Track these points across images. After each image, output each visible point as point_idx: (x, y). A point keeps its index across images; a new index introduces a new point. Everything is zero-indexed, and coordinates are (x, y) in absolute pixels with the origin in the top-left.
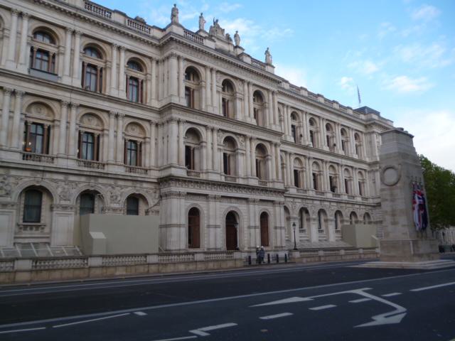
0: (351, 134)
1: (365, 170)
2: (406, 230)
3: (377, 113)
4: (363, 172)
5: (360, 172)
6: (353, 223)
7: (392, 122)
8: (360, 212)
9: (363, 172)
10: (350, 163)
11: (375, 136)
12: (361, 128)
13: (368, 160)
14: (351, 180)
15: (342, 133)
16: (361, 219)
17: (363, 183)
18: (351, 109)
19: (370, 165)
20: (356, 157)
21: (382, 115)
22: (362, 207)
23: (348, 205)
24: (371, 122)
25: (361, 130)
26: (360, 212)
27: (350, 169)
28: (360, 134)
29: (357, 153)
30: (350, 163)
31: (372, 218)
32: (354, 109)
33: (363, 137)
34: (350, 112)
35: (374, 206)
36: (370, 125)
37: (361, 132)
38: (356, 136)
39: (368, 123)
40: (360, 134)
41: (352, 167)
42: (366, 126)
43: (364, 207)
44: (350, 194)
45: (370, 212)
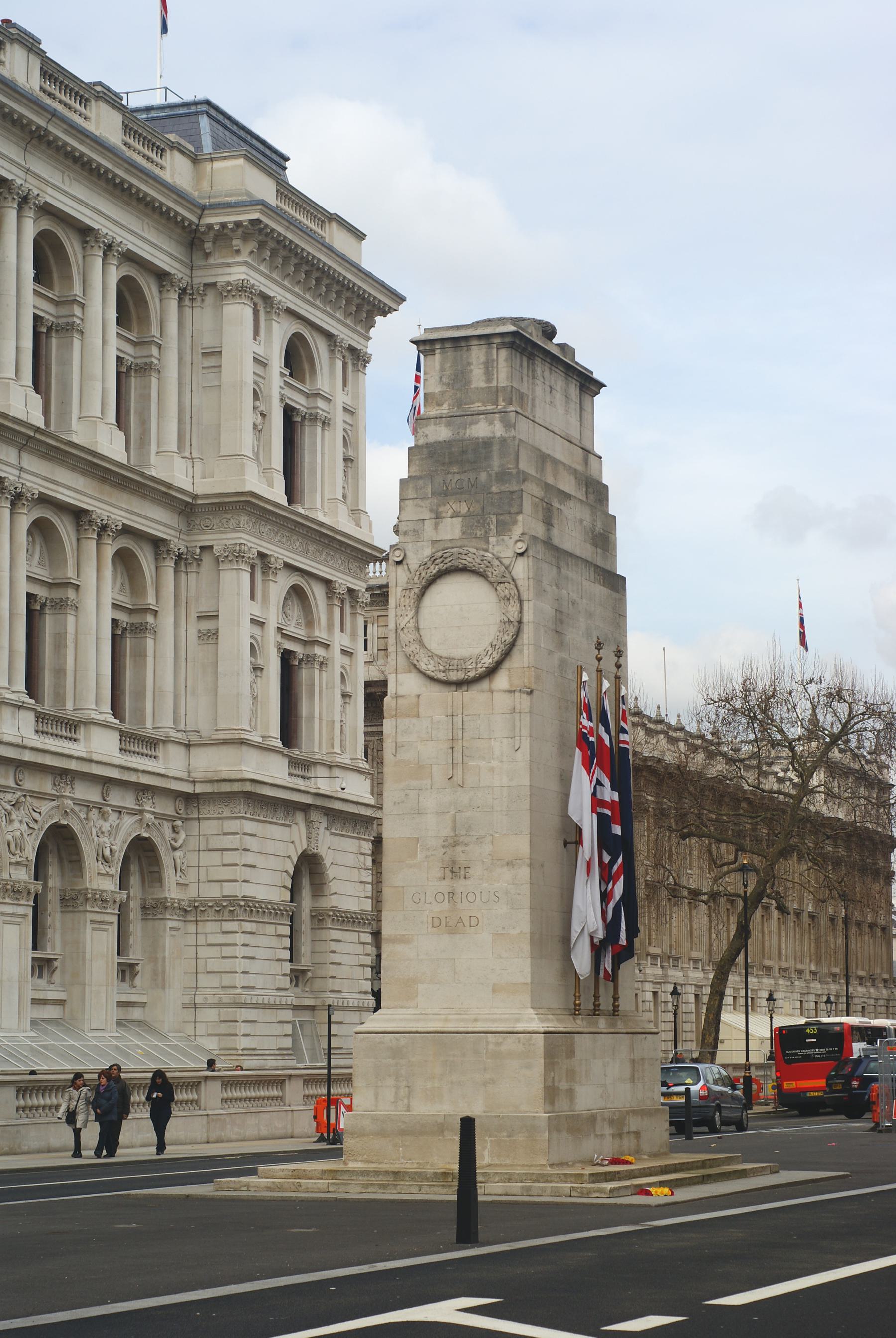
0: (98, 288)
1: (157, 544)
2: (519, 967)
3: (271, 160)
4: (145, 558)
5: (124, 559)
6: (53, 898)
7: (361, 236)
8: (106, 836)
9: (145, 558)
10: (72, 487)
11: (249, 312)
12: (161, 252)
13: (179, 474)
14: (60, 605)
15: (42, 274)
16: (101, 879)
17: (140, 630)
18: (112, 99)
19: (188, 509)
20: (111, 445)
21: (295, 176)
22: (116, 798)
23: (31, 783)
24: (230, 219)
25: (163, 262)
26: (106, 836)
27: (65, 528)
28: (150, 288)
29: (121, 421)
30: (72, 487)
31: (170, 876)
32: (135, 102)
33: (165, 309)
34: (105, 125)
35: (190, 799)
36: (223, 235)
37: (162, 277)
38: (130, 307)
39: (214, 220)
40: (150, 288)
41: (78, 515)
42: (194, 240)
43: (128, 801)
44: (47, 706)
45: (162, 837)
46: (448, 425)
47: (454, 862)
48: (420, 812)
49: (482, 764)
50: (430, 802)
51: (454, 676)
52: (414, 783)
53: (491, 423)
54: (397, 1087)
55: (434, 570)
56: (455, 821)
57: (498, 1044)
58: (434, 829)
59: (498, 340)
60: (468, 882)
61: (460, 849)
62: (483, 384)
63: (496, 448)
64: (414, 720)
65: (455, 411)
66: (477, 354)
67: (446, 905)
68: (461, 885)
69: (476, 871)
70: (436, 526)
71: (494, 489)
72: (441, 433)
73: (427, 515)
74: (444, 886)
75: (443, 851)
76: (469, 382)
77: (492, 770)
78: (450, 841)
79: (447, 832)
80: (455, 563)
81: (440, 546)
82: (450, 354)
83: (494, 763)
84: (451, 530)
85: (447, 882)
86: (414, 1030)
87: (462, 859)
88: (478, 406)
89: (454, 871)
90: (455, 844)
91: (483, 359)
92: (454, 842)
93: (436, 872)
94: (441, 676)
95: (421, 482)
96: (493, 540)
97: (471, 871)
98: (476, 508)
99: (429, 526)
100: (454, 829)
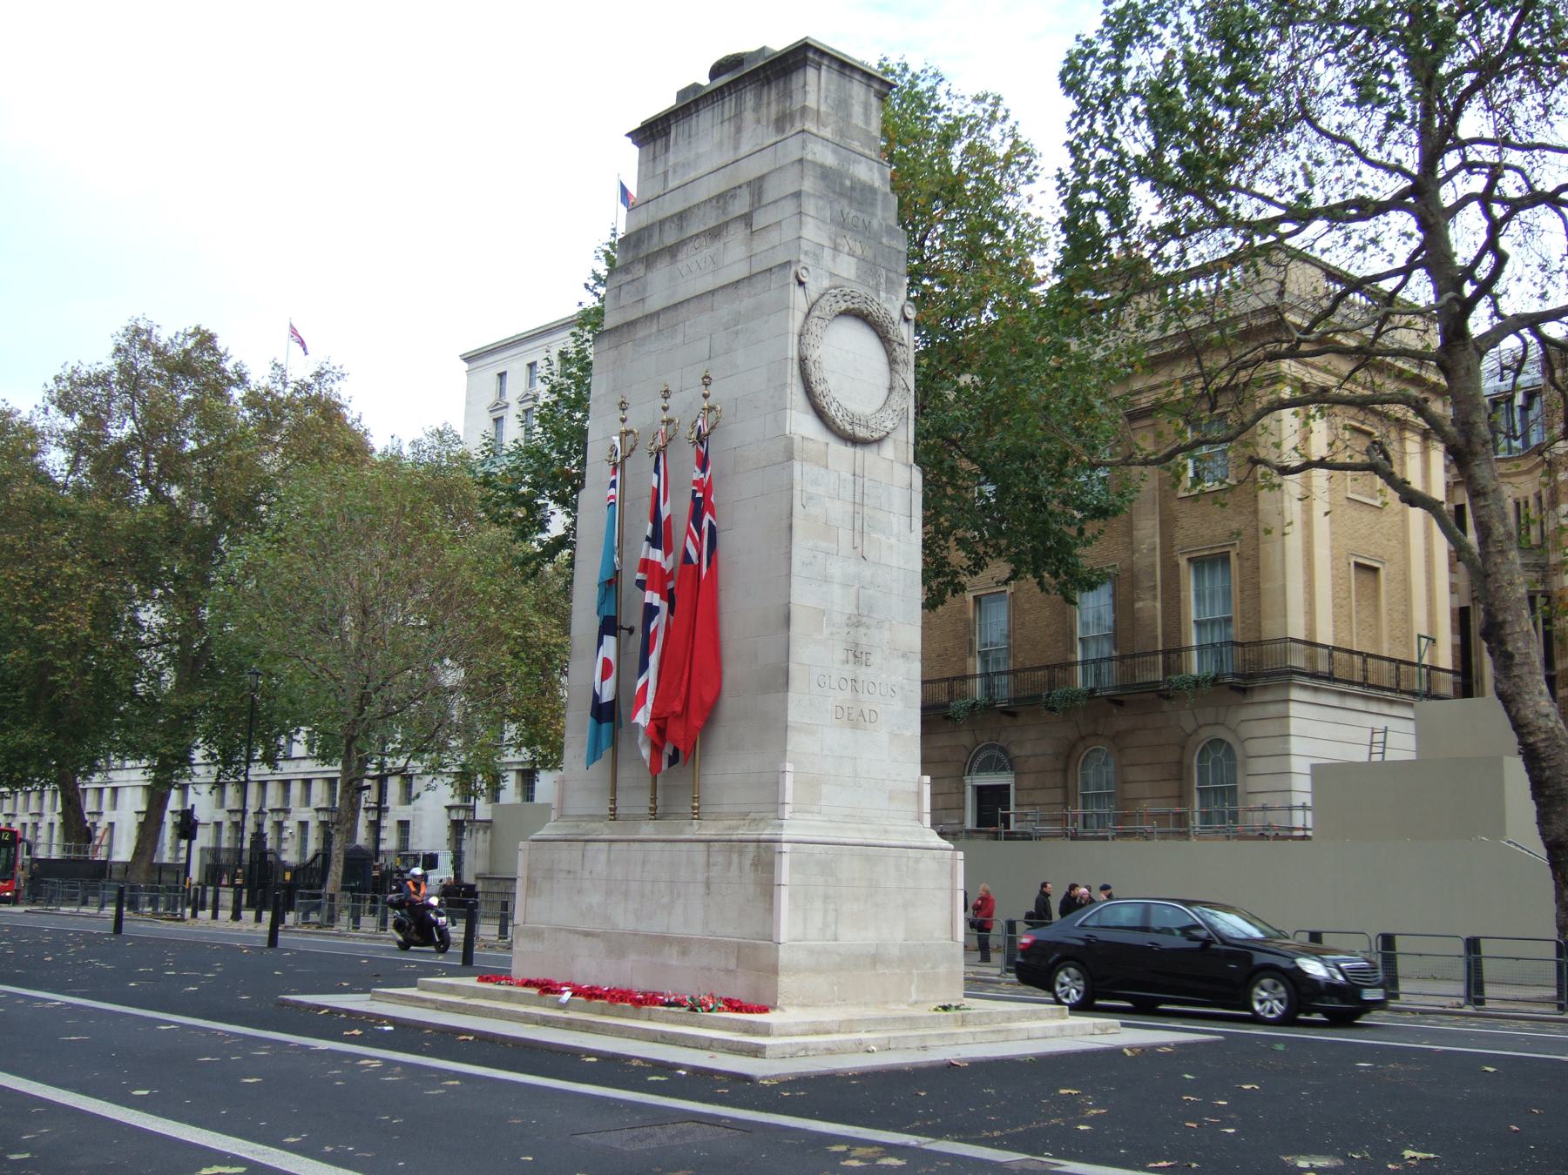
46: (834, 152)
47: (857, 645)
48: (827, 580)
49: (883, 538)
50: (836, 569)
51: (861, 433)
52: (822, 544)
53: (871, 170)
54: (826, 911)
55: (843, 306)
56: (858, 598)
57: (917, 860)
58: (840, 603)
59: (876, 86)
60: (870, 670)
61: (862, 630)
62: (861, 124)
63: (880, 198)
64: (823, 471)
65: (837, 140)
66: (857, 90)
67: (848, 694)
68: (863, 673)
69: (876, 659)
70: (834, 260)
71: (884, 240)
72: (828, 158)
73: (826, 243)
74: (848, 671)
75: (846, 630)
76: (849, 115)
77: (891, 547)
78: (854, 620)
79: (851, 609)
80: (863, 306)
81: (837, 282)
82: (835, 76)
83: (893, 540)
84: (847, 268)
85: (850, 667)
86: (842, 840)
87: (863, 641)
88: (856, 145)
89: (857, 655)
90: (858, 625)
91: (862, 98)
92: (856, 622)
93: (840, 655)
94: (848, 428)
95: (821, 203)
96: (882, 294)
97: (872, 659)
98: (869, 254)
99: (827, 253)
100: (858, 607)
